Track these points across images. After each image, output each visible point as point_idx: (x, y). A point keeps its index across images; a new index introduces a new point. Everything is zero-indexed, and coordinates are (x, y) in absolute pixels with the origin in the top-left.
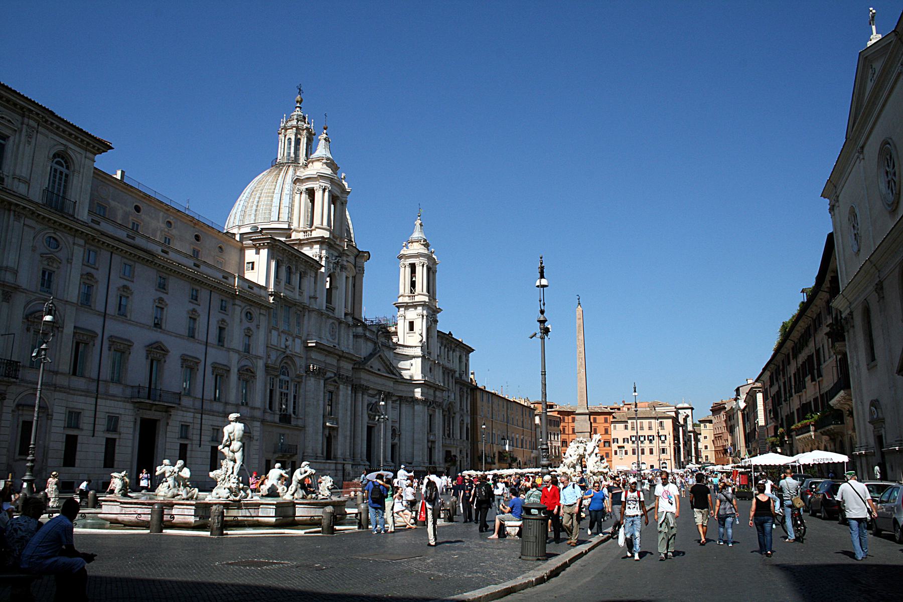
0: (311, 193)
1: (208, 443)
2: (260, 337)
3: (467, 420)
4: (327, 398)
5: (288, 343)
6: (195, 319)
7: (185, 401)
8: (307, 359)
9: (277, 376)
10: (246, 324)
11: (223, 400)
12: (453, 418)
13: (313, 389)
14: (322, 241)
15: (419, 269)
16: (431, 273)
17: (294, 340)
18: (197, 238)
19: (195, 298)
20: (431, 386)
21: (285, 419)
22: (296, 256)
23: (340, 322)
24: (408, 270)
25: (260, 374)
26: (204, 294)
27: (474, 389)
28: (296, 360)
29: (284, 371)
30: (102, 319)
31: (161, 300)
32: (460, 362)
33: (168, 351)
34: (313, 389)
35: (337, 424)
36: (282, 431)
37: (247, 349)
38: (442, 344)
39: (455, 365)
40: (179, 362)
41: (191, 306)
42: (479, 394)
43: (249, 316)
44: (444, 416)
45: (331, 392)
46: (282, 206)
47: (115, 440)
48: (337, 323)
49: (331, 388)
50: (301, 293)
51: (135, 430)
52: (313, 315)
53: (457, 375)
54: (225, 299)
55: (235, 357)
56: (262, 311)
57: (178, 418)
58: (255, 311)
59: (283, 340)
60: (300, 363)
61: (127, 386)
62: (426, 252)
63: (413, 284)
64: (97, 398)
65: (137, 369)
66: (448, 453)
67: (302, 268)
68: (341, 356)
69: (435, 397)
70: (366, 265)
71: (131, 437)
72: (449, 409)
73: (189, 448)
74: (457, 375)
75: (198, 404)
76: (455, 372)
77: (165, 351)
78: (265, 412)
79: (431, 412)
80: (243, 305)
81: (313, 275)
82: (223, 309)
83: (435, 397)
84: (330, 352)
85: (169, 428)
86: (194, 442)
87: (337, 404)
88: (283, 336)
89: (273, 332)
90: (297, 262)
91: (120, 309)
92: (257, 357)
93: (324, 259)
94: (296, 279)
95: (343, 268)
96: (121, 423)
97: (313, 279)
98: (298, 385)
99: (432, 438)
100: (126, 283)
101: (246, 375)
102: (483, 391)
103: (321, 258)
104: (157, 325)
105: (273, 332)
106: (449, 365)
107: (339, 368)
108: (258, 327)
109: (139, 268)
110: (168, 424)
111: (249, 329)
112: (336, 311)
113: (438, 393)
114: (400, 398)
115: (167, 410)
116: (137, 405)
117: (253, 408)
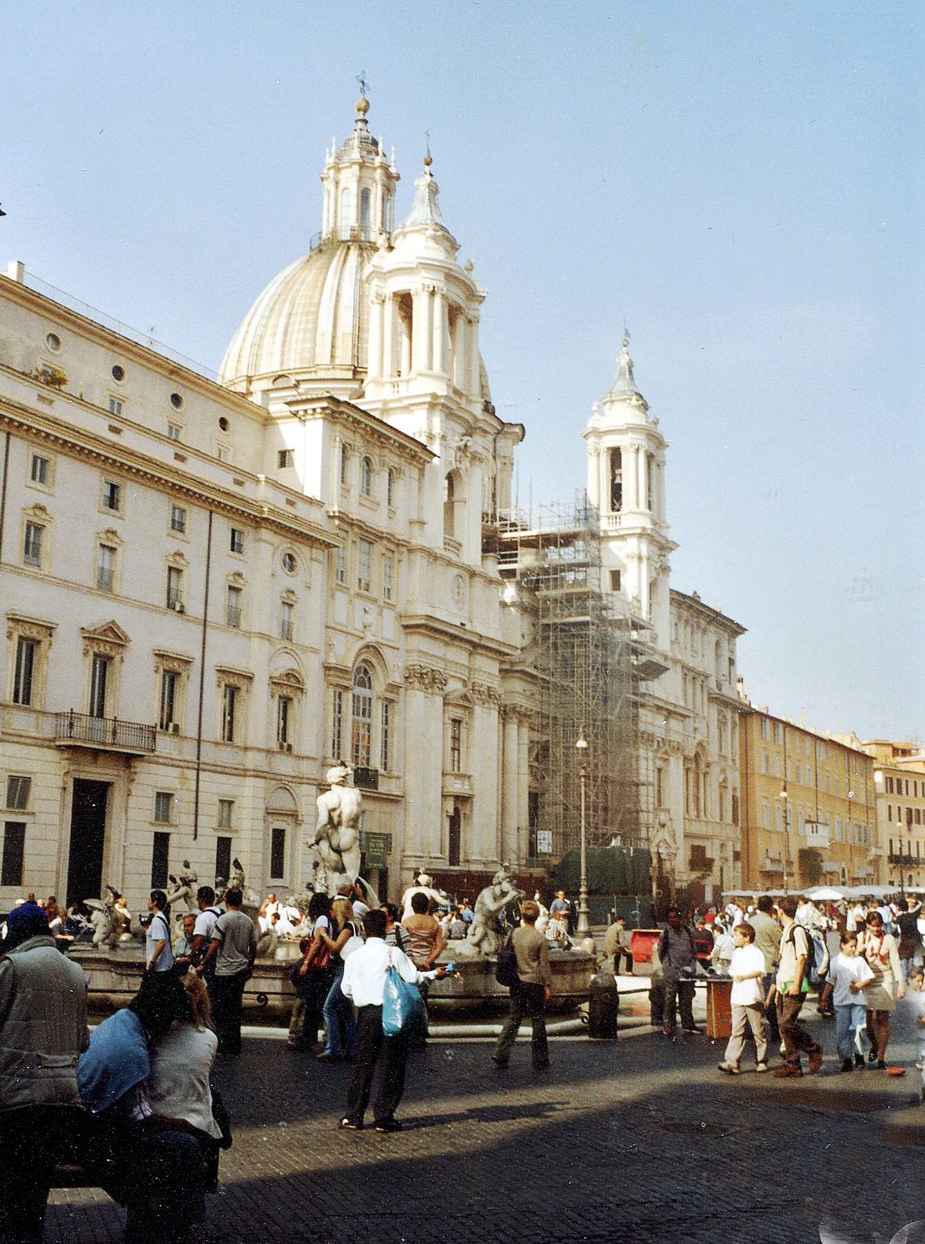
1: (213, 833)
2: (311, 609)
3: (735, 779)
4: (449, 733)
5: (369, 619)
6: (179, 571)
7: (165, 745)
10: (286, 580)
12: (705, 774)
13: (422, 715)
15: (627, 459)
16: (654, 466)
17: (380, 614)
18: (176, 400)
19: (178, 526)
22: (381, 435)
23: (473, 574)
24: (605, 461)
25: (314, 682)
26: (196, 518)
27: (747, 714)
28: (386, 652)
29: (364, 677)
32: (718, 656)
33: (127, 640)
34: (422, 715)
35: (471, 789)
37: (287, 633)
38: (680, 618)
39: (705, 663)
40: (151, 662)
41: (173, 545)
42: (755, 723)
43: (290, 562)
44: (687, 770)
45: (457, 722)
46: (339, 333)
47: (23, 825)
48: (466, 576)
50: (392, 514)
51: (63, 806)
52: (418, 558)
53: (712, 684)
54: (238, 527)
56: (317, 553)
57: (151, 778)
58: (303, 552)
59: (359, 614)
62: (643, 422)
63: (616, 491)
65: (65, 679)
67: (393, 460)
68: (476, 646)
69: (668, 730)
70: (520, 452)
72: (697, 755)
73: (173, 842)
74: (712, 684)
75: (189, 752)
76: (707, 677)
79: (659, 763)
80: (277, 539)
81: (415, 473)
82: (235, 546)
83: (668, 730)
84: (454, 637)
85: (132, 802)
86: (183, 829)
88: (359, 604)
89: (338, 595)
91: (27, 552)
92: (306, 649)
93: (437, 441)
94: (380, 481)
95: (475, 458)
96: (34, 792)
97: (415, 484)
98: (388, 703)
101: (288, 690)
102: (763, 716)
103: (431, 437)
104: (105, 583)
105: (338, 595)
106: (691, 663)
109: (64, 468)
112: (464, 549)
113: (675, 724)
115: (128, 760)
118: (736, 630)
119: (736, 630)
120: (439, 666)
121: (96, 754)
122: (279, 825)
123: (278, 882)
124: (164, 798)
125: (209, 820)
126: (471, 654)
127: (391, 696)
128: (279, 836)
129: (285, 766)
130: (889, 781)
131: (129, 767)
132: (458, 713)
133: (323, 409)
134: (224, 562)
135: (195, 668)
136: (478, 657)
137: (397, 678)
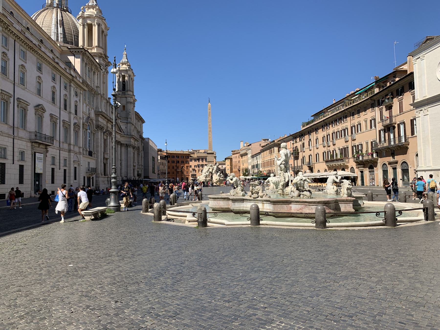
0: (90, 27)
8: (96, 121)
9: (86, 130)
11: (68, 142)
14: (100, 56)
20: (134, 139)
21: (90, 154)
30: (13, 86)
31: (39, 77)
36: (89, 160)
40: (49, 118)
49: (105, 137)
55: (72, 116)
58: (79, 91)
60: (94, 122)
61: (27, 131)
64: (14, 139)
66: (138, 171)
71: (30, 163)
73: (55, 170)
77: (44, 110)
78: (83, 150)
80: (74, 87)
82: (65, 87)
84: (105, 118)
87: (107, 146)
90: (92, 65)
99: (135, 165)
100: (23, 63)
104: (39, 92)
107: (107, 127)
108: (80, 100)
109: (29, 54)
110: (46, 156)
111: (76, 101)
114: (122, 145)
116: (33, 143)
117: (80, 147)
118: (143, 122)
119: (143, 122)
120: (102, 125)
121: (40, 144)
122: (76, 166)
123: (75, 181)
124: (53, 158)
125: (62, 165)
126: (107, 123)
127: (94, 132)
128: (75, 168)
129: (77, 149)
130: (161, 157)
131: (46, 148)
132: (105, 137)
133: (82, 52)
134: (63, 92)
135: (58, 121)
136: (108, 124)
137: (95, 128)
